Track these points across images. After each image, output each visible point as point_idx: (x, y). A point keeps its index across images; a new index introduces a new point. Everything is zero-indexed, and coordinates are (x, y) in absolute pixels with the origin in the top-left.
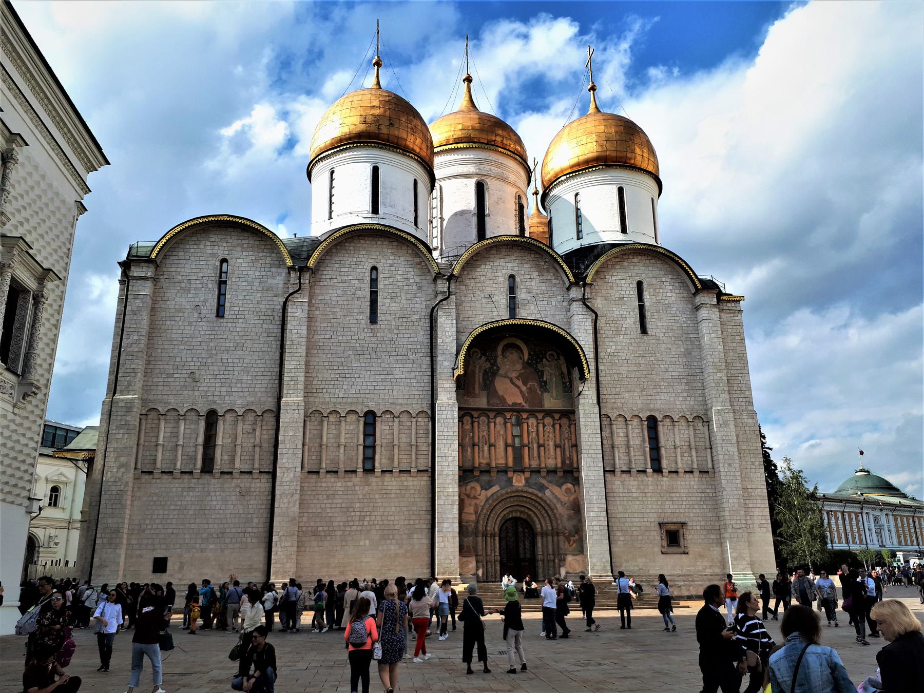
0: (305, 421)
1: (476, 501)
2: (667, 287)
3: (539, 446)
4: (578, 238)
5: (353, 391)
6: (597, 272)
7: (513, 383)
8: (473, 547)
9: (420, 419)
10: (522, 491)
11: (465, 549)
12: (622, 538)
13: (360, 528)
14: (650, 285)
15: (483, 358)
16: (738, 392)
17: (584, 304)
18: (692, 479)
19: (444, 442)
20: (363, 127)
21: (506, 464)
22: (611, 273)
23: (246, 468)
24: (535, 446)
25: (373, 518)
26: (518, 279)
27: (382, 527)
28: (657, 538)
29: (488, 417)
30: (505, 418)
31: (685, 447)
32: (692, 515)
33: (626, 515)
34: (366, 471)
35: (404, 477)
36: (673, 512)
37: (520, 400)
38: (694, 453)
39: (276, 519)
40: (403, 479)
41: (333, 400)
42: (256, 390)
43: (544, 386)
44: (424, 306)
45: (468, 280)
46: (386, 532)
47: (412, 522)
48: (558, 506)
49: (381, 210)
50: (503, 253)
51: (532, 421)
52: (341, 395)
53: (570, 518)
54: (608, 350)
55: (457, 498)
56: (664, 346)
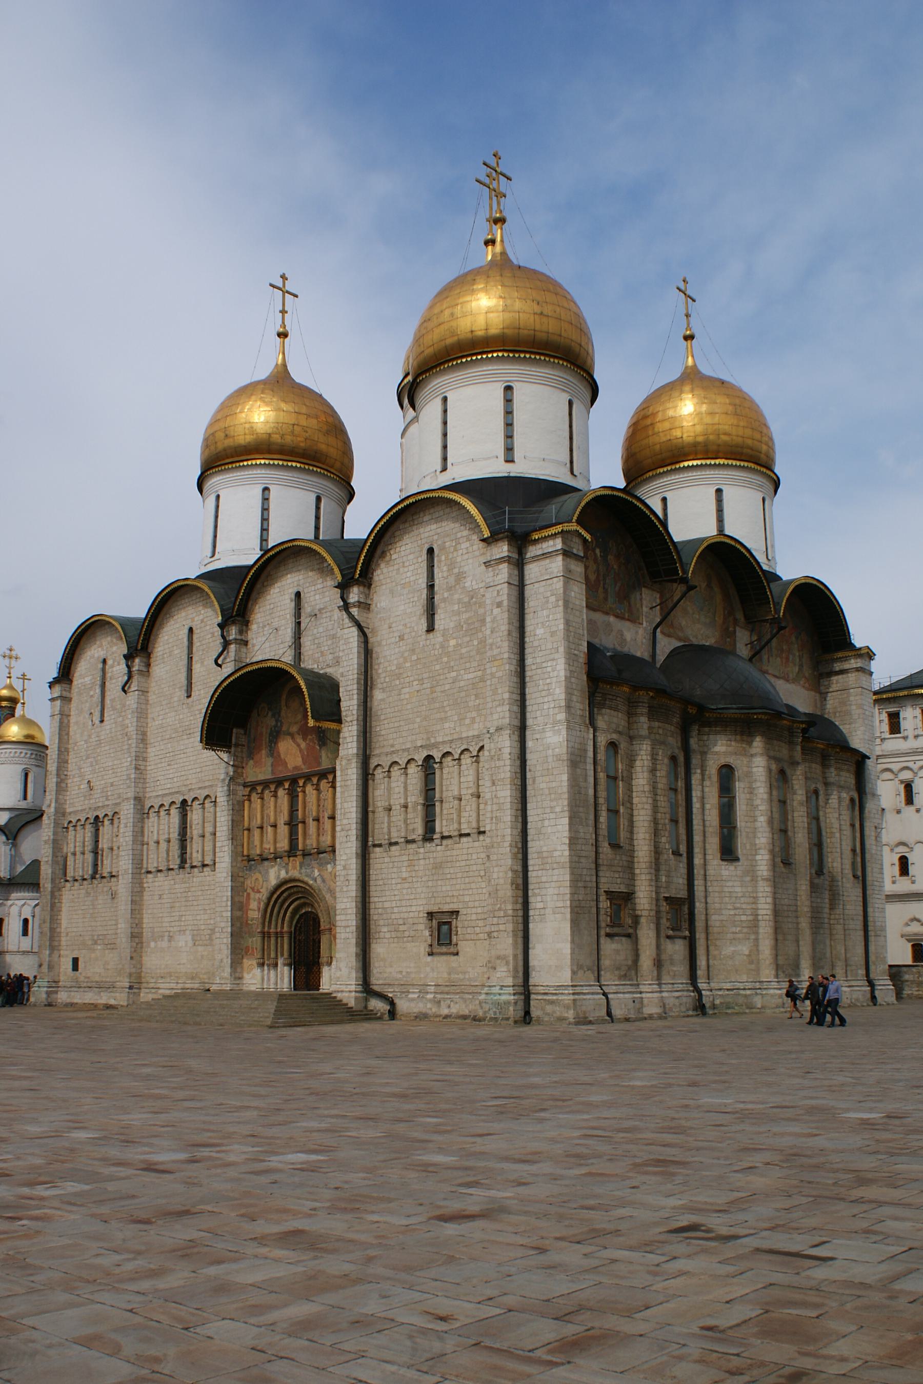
1: (258, 895)
2: (464, 546)
12: (388, 935)
14: (443, 548)
15: (270, 714)
16: (544, 693)
18: (471, 845)
22: (398, 549)
32: (467, 899)
38: (474, 806)
40: (206, 873)
41: (165, 792)
42: (121, 791)
50: (290, 565)
52: (169, 786)
54: (389, 669)
55: (229, 894)
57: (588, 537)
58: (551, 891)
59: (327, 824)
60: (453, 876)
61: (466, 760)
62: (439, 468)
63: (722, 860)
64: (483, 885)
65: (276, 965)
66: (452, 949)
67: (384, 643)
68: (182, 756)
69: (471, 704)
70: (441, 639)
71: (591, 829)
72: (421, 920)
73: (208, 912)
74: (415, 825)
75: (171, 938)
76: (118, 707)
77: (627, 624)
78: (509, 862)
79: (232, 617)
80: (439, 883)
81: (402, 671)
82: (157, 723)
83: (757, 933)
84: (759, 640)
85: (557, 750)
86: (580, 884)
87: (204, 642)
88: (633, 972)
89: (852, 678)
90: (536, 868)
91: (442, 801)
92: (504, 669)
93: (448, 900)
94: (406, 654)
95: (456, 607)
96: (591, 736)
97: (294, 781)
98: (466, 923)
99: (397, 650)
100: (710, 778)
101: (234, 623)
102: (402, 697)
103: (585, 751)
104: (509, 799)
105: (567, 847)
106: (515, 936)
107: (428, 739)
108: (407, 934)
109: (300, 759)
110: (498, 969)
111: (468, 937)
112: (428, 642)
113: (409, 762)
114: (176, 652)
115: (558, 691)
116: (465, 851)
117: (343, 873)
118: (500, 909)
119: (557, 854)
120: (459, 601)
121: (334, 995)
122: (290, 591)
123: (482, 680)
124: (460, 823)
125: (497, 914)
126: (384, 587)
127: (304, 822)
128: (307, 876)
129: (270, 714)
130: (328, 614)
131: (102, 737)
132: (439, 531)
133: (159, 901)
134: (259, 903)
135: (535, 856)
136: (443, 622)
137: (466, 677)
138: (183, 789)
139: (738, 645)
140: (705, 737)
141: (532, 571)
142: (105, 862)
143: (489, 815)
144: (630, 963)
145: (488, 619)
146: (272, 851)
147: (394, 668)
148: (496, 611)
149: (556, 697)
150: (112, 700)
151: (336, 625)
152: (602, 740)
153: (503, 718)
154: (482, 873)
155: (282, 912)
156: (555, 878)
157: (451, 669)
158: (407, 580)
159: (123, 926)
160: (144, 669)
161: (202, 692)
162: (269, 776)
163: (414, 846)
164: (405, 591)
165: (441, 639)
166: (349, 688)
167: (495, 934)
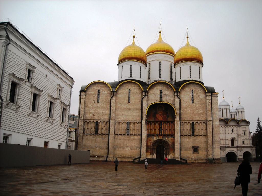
0: (115, 124)
1: (150, 142)
3: (166, 130)
4: (180, 78)
6: (182, 88)
7: (161, 116)
10: (161, 139)
11: (148, 151)
12: (184, 150)
14: (195, 91)
17: (177, 96)
20: (129, 56)
21: (158, 133)
23: (104, 133)
24: (165, 129)
26: (162, 91)
29: (154, 123)
30: (158, 123)
32: (201, 145)
34: (127, 135)
35: (135, 136)
36: (197, 144)
37: (162, 119)
38: (202, 131)
39: (109, 144)
41: (121, 120)
43: (168, 116)
44: (140, 98)
45: (150, 91)
48: (169, 143)
51: (165, 124)
52: (122, 118)
53: (172, 145)
55: (146, 141)
56: (197, 106)
58: (216, 145)
62: (189, 76)
64: (204, 143)
70: (195, 105)
75: (123, 148)
82: (118, 106)
95: (198, 100)
107: (192, 120)
110: (210, 155)
113: (188, 123)
120: (199, 100)
122: (159, 89)
123: (203, 112)
127: (163, 130)
138: (127, 120)
141: (213, 98)
142: (100, 131)
148: (209, 103)
157: (197, 110)
159: (111, 145)
164: (187, 95)
165: (195, 105)
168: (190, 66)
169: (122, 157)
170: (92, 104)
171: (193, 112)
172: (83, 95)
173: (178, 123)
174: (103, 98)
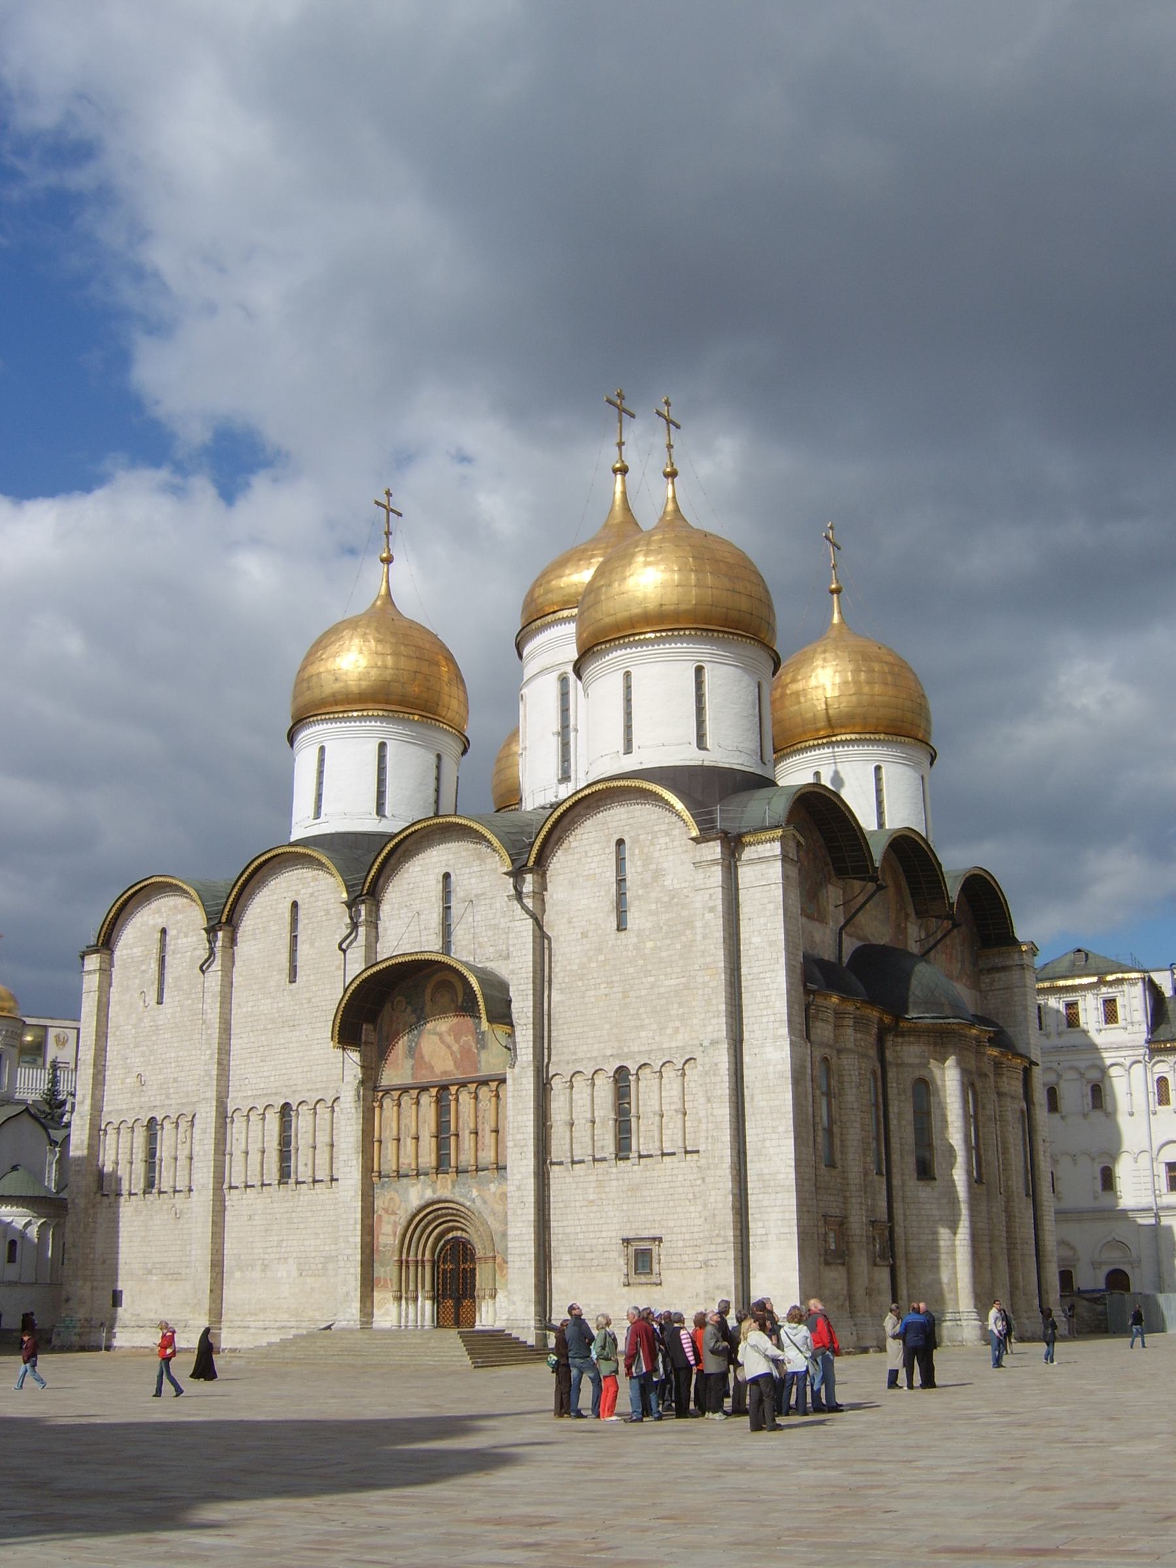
1: (393, 1218)
2: (662, 841)
3: (471, 1133)
5: (272, 1079)
7: (443, 1042)
8: (391, 1280)
9: (336, 1109)
12: (570, 1264)
13: (278, 1256)
14: (636, 841)
16: (762, 1006)
18: (676, 1165)
19: (347, 1140)
22: (578, 837)
24: (467, 1132)
25: (290, 1243)
26: (453, 878)
27: (299, 1255)
28: (619, 1261)
31: (670, 1113)
32: (671, 1224)
33: (578, 1230)
37: (449, 1066)
38: (680, 1124)
40: (319, 1191)
41: (255, 1092)
42: (189, 1089)
45: (393, 895)
46: (301, 1260)
47: (327, 1248)
48: (490, 1220)
49: (324, 810)
52: (262, 1086)
54: (568, 968)
55: (359, 1216)
57: (802, 840)
59: (488, 1138)
60: (654, 1199)
61: (669, 1073)
62: (621, 747)
63: (919, 1179)
64: (692, 1209)
65: (416, 1299)
66: (654, 1279)
67: (562, 939)
68: (283, 1051)
69: (673, 1012)
70: (635, 940)
71: (811, 1150)
72: (614, 1247)
73: (321, 1236)
74: (605, 1143)
75: (265, 1267)
76: (185, 987)
77: (817, 924)
78: (729, 1185)
79: (361, 895)
80: (637, 1206)
81: (585, 971)
82: (245, 1010)
83: (954, 1260)
84: (928, 936)
85: (779, 1066)
86: (805, 1209)
87: (314, 920)
88: (847, 1304)
89: (1015, 975)
90: (756, 1191)
91: (639, 1118)
92: (719, 980)
93: (648, 1225)
94: (591, 953)
95: (653, 906)
96: (809, 1052)
97: (444, 1088)
98: (671, 1250)
99: (579, 948)
100: (904, 1092)
101: (363, 902)
102: (587, 1000)
103: (805, 1067)
104: (728, 1118)
105: (793, 1170)
106: (735, 1264)
107: (620, 1048)
108: (595, 1262)
109: (452, 1063)
111: (672, 1265)
112: (619, 942)
114: (273, 928)
115: (778, 1004)
116: (668, 1172)
117: (516, 1194)
118: (718, 1235)
119: (781, 1176)
120: (658, 901)
121: (506, 1332)
122: (437, 871)
124: (662, 1141)
125: (714, 1241)
126: (561, 877)
127: (457, 1135)
128: (462, 1196)
129: (409, 1009)
130: (488, 901)
131: (160, 1023)
132: (631, 821)
133: (250, 1223)
134: (395, 1227)
135: (755, 1178)
136: (637, 921)
137: (667, 983)
139: (909, 941)
140: (899, 1048)
141: (746, 874)
142: (164, 1174)
143: (703, 1134)
144: (845, 1292)
145: (698, 924)
146: (413, 1167)
147: (575, 967)
148: (709, 916)
149: (776, 1011)
150: (177, 979)
151: (498, 914)
152: (818, 1054)
153: (719, 1030)
154: (691, 1196)
155: (425, 1236)
156: (779, 1202)
158: (591, 872)
160: (228, 945)
161: (312, 977)
162: (408, 1081)
163: (604, 1164)
165: (635, 940)
166: (521, 987)
167: (713, 1263)
168: (627, 675)
169: (261, 1324)
170: (134, 1016)
171: (625, 994)
172: (90, 972)
173: (524, 1081)
174: (180, 976)
